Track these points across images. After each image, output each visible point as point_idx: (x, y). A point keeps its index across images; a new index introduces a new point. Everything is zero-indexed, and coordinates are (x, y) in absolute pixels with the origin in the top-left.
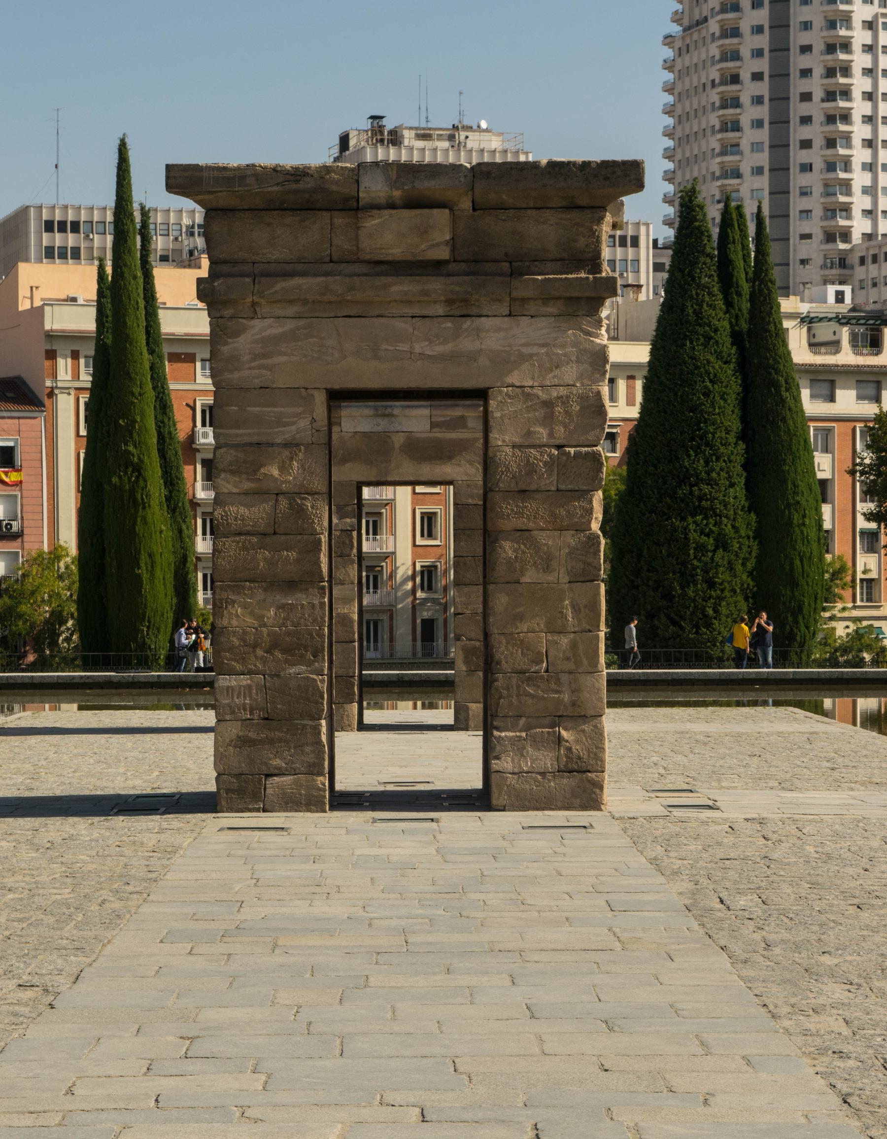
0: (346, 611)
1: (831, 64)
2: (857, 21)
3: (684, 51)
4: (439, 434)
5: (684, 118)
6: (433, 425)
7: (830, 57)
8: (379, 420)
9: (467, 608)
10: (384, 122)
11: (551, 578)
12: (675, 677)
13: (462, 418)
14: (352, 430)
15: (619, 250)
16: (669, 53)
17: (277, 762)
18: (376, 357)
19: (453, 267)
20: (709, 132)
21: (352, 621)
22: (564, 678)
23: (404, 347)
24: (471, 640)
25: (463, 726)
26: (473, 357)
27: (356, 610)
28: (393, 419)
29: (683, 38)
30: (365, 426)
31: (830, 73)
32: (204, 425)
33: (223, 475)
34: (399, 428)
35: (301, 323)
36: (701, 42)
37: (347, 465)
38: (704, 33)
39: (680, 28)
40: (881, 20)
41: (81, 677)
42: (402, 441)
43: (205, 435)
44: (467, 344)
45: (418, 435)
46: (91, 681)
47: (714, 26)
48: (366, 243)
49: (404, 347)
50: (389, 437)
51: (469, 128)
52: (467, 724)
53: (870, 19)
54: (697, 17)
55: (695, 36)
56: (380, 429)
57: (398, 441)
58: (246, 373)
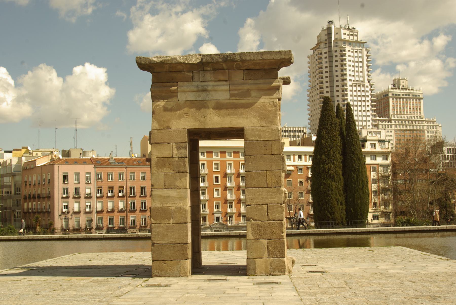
0: (181, 205)
1: (343, 94)
2: (348, 85)
3: (311, 92)
5: (312, 107)
6: (231, 96)
7: (343, 92)
8: (200, 93)
9: (253, 202)
12: (337, 232)
13: (248, 91)
14: (184, 100)
15: (299, 133)
16: (308, 93)
20: (317, 109)
21: (185, 211)
24: (256, 220)
25: (252, 273)
27: (189, 203)
28: (208, 93)
29: (311, 90)
30: (191, 97)
31: (343, 96)
32: (201, 168)
34: (212, 98)
36: (315, 90)
37: (182, 119)
38: (316, 88)
39: (310, 88)
40: (353, 85)
41: (129, 235)
42: (213, 105)
43: (202, 171)
45: (223, 102)
46: (132, 236)
47: (318, 87)
50: (205, 103)
52: (255, 272)
53: (351, 84)
54: (314, 85)
55: (314, 89)
56: (200, 99)
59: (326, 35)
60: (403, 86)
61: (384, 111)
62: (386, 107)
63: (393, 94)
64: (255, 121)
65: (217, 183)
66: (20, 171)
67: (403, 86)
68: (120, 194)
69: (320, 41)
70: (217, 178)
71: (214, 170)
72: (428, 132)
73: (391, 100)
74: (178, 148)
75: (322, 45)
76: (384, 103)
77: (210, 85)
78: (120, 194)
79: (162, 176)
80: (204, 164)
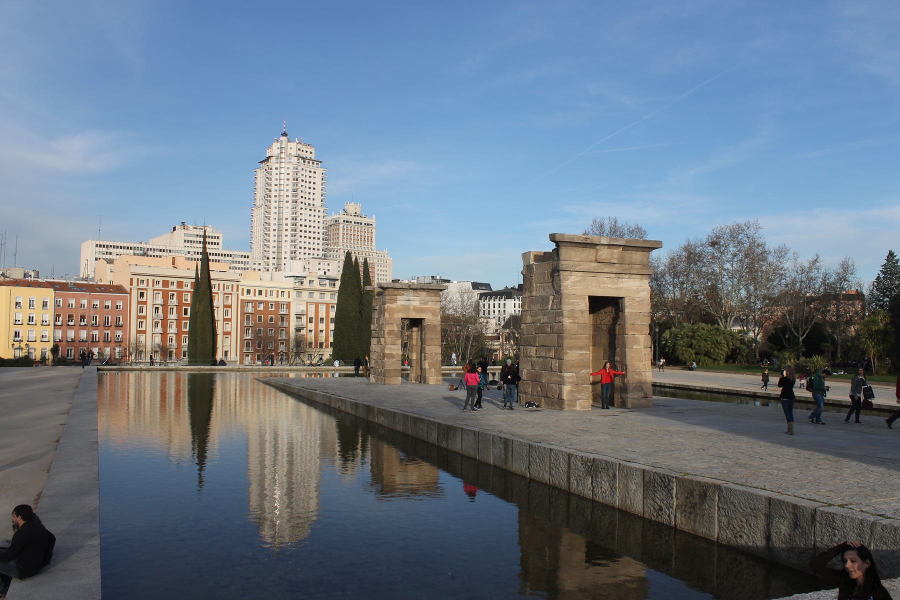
4: (423, 306)
6: (420, 303)
10: (185, 224)
11: (639, 347)
17: (579, 396)
18: (600, 288)
19: (616, 265)
22: (643, 373)
23: (606, 285)
26: (621, 288)
30: (403, 303)
33: (566, 318)
35: (582, 278)
43: (171, 302)
44: (620, 285)
48: (598, 258)
49: (606, 285)
51: (207, 227)
57: (412, 307)
58: (569, 290)
59: (278, 148)
60: (356, 213)
61: (333, 239)
62: (336, 234)
63: (344, 221)
64: (430, 315)
65: (186, 316)
66: (226, 324)
67: (356, 213)
68: (82, 324)
69: (269, 155)
70: (186, 310)
71: (184, 302)
72: (378, 266)
73: (341, 226)
74: (398, 328)
75: (273, 160)
76: (333, 230)
77: (412, 298)
78: (82, 324)
79: (390, 339)
80: (173, 295)
